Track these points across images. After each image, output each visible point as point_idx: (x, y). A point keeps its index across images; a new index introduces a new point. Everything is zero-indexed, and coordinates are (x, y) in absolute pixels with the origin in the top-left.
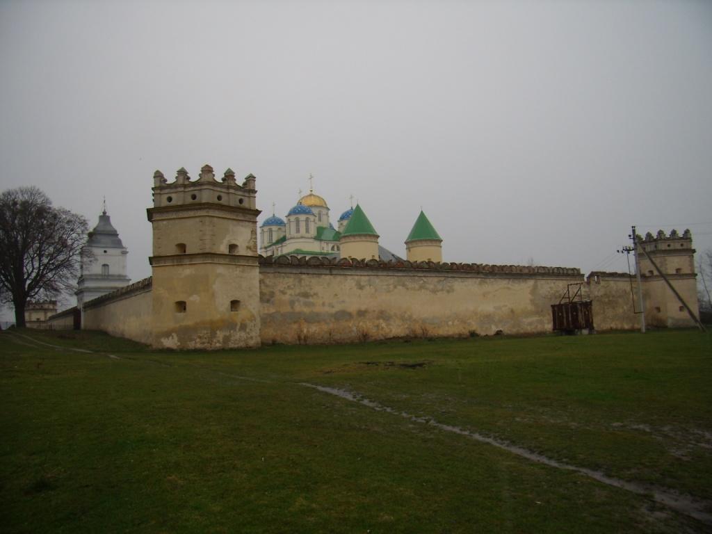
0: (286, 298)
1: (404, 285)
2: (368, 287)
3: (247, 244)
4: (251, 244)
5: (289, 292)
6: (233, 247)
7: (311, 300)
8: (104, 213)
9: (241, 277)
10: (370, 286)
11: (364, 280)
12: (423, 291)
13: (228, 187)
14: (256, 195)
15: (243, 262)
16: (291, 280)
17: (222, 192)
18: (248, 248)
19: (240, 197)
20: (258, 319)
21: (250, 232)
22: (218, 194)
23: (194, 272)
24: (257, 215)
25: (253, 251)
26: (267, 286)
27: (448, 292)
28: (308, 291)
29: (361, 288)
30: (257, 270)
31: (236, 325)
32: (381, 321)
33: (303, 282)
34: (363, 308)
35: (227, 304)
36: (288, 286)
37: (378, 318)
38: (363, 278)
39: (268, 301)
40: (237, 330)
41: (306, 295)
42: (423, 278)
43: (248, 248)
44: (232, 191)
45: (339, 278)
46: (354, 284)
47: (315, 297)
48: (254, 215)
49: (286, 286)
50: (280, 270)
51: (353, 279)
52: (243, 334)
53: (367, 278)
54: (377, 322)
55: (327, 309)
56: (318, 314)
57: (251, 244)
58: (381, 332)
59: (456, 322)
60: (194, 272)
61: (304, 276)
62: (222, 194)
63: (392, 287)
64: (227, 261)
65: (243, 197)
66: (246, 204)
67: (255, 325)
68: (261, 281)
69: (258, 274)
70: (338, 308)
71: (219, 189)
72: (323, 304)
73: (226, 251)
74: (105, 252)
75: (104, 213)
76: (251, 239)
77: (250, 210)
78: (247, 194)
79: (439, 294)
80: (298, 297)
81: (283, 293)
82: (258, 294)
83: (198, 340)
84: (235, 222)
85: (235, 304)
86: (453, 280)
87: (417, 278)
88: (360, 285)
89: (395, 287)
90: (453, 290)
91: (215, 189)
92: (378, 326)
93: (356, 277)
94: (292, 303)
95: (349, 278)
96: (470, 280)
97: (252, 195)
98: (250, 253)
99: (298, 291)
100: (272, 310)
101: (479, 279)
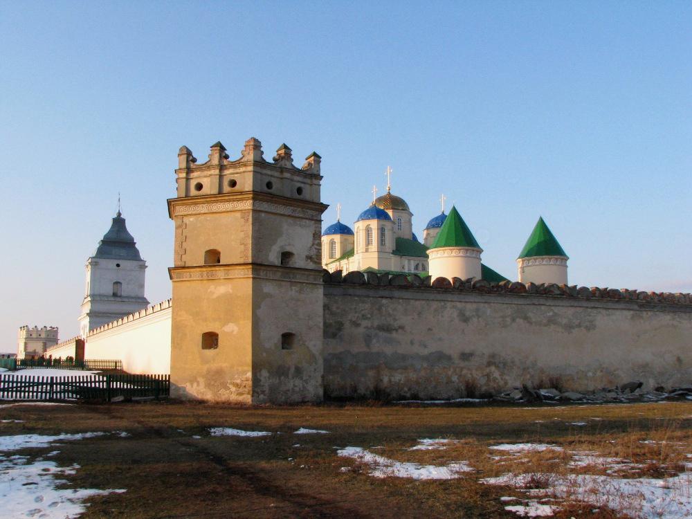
0: (361, 330)
1: (526, 318)
2: (475, 320)
3: (307, 253)
4: (313, 252)
5: (365, 323)
6: (286, 256)
7: (394, 335)
8: (119, 214)
9: (298, 300)
10: (479, 317)
11: (470, 308)
12: (552, 326)
13: (282, 170)
14: (321, 182)
15: (300, 278)
16: (367, 306)
17: (271, 176)
18: (309, 258)
19: (299, 185)
20: (321, 362)
21: (312, 235)
22: (267, 180)
23: (231, 291)
24: (322, 211)
25: (315, 263)
26: (332, 314)
27: (588, 329)
29: (466, 320)
30: (321, 291)
31: (289, 369)
32: (493, 368)
34: (467, 351)
35: (277, 338)
36: (363, 316)
37: (489, 364)
38: (469, 306)
39: (334, 336)
40: (290, 376)
41: (387, 329)
42: (553, 308)
43: (309, 258)
44: (287, 175)
45: (435, 305)
46: (455, 314)
47: (400, 331)
48: (316, 210)
49: (360, 315)
50: (351, 291)
51: (454, 307)
52: (298, 382)
53: (475, 306)
54: (487, 370)
55: (417, 349)
56: (404, 357)
57: (313, 252)
58: (492, 384)
59: (599, 374)
60: (231, 291)
61: (384, 301)
62: (273, 180)
63: (508, 319)
65: (302, 185)
66: (307, 195)
67: (315, 370)
68: (326, 307)
69: (321, 296)
70: (433, 348)
71: (269, 172)
72: (412, 343)
73: (277, 262)
74: (118, 265)
75: (119, 214)
76: (313, 245)
77: (313, 203)
78: (308, 181)
79: (575, 331)
81: (357, 325)
82: (321, 325)
83: (233, 389)
84: (290, 220)
85: (287, 339)
86: (595, 311)
87: (543, 307)
88: (464, 315)
89: (513, 320)
90: (594, 327)
91: (265, 171)
92: (488, 375)
93: (459, 304)
94: (368, 339)
95: (449, 304)
96: (618, 313)
97: (315, 182)
98: (311, 266)
99: (376, 323)
100: (340, 349)
101: (632, 312)
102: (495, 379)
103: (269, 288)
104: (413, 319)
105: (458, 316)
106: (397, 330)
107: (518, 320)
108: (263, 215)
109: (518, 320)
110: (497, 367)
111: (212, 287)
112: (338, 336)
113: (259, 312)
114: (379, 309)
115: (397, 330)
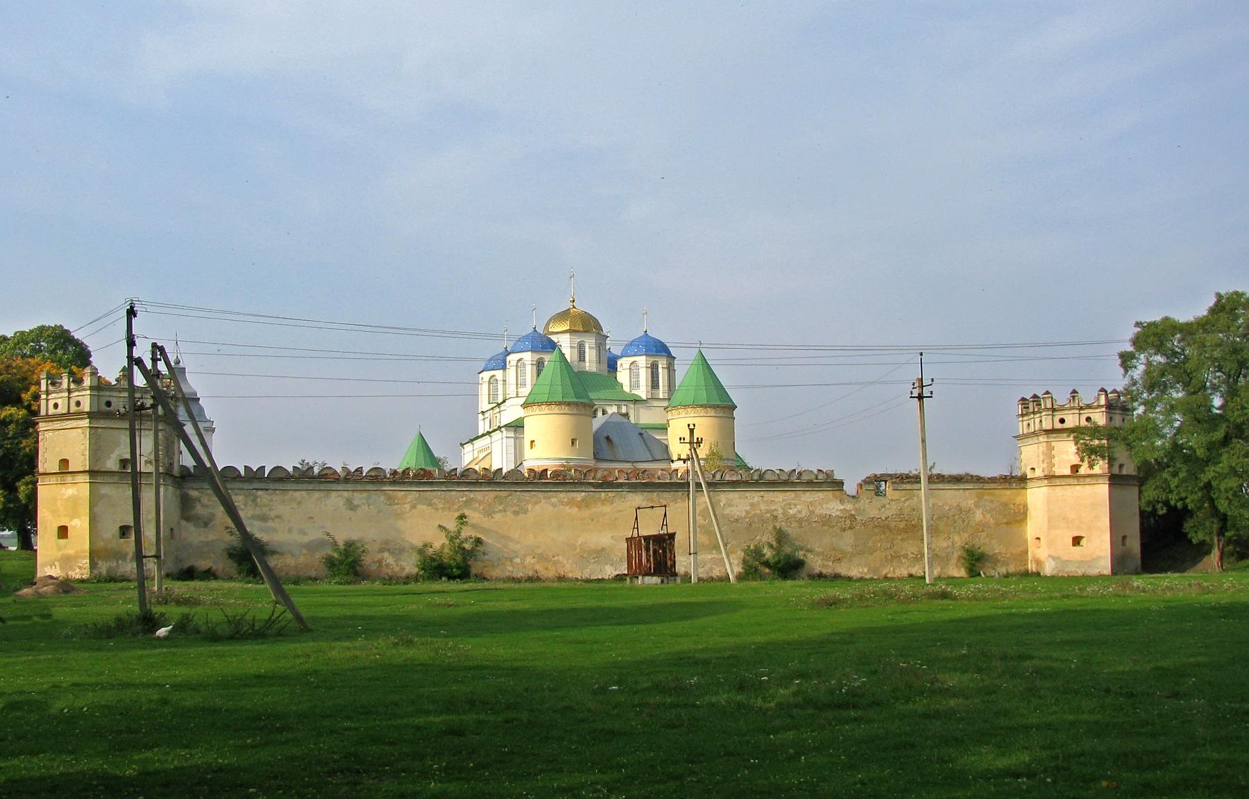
7: (270, 524)
11: (359, 498)
17: (110, 396)
22: (104, 400)
23: (76, 493)
28: (268, 512)
29: (352, 507)
32: (386, 554)
33: (259, 499)
35: (115, 529)
37: (381, 550)
40: (128, 561)
42: (466, 493)
45: (316, 495)
46: (341, 504)
47: (276, 520)
51: (339, 496)
53: (365, 495)
61: (260, 493)
62: (111, 399)
64: (116, 479)
80: (252, 521)
83: (78, 570)
89: (414, 507)
93: (346, 494)
95: (334, 494)
102: (387, 566)
103: (105, 490)
104: (292, 508)
105: (344, 505)
106: (273, 520)
107: (419, 507)
108: (100, 430)
109: (419, 507)
110: (391, 553)
111: (64, 489)
112: (209, 526)
113: (96, 509)
114: (254, 501)
115: (273, 520)
